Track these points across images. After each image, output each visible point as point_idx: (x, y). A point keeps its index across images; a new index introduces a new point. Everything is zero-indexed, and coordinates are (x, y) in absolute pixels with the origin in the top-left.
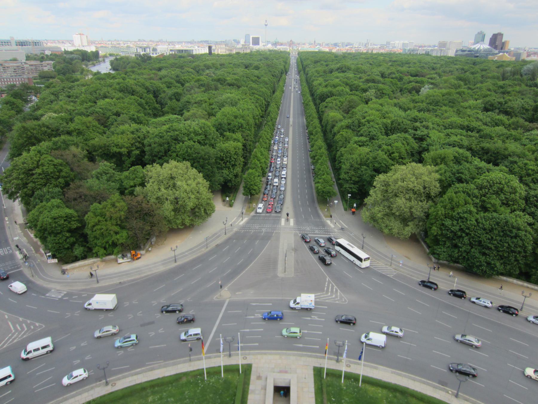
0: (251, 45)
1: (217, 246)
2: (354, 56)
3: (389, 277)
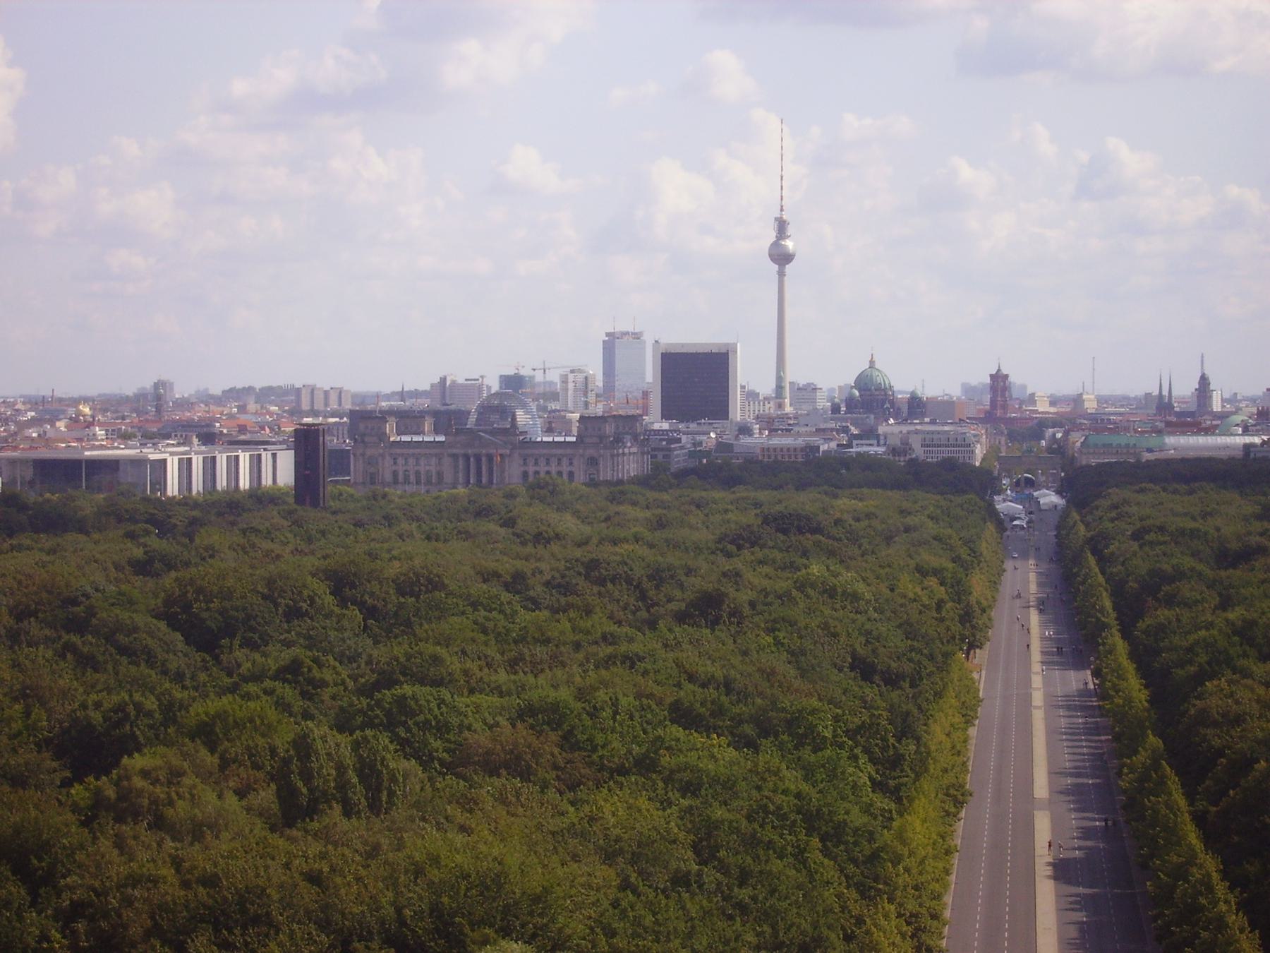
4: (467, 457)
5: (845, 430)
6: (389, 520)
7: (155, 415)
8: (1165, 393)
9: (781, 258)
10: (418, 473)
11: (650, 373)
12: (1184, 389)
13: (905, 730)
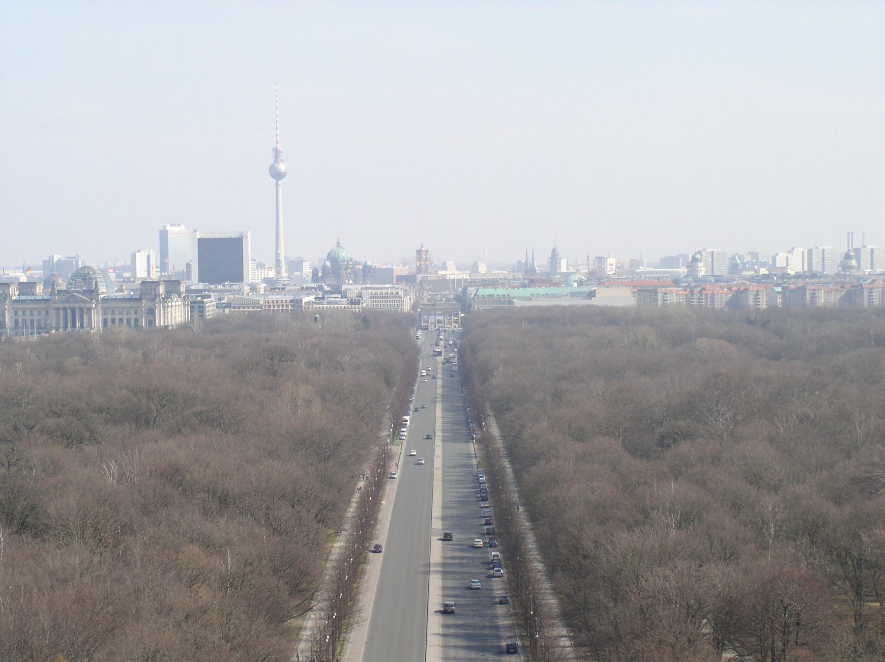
0: (195, 283)
4: (65, 309)
5: (321, 288)
8: (530, 260)
10: (32, 322)
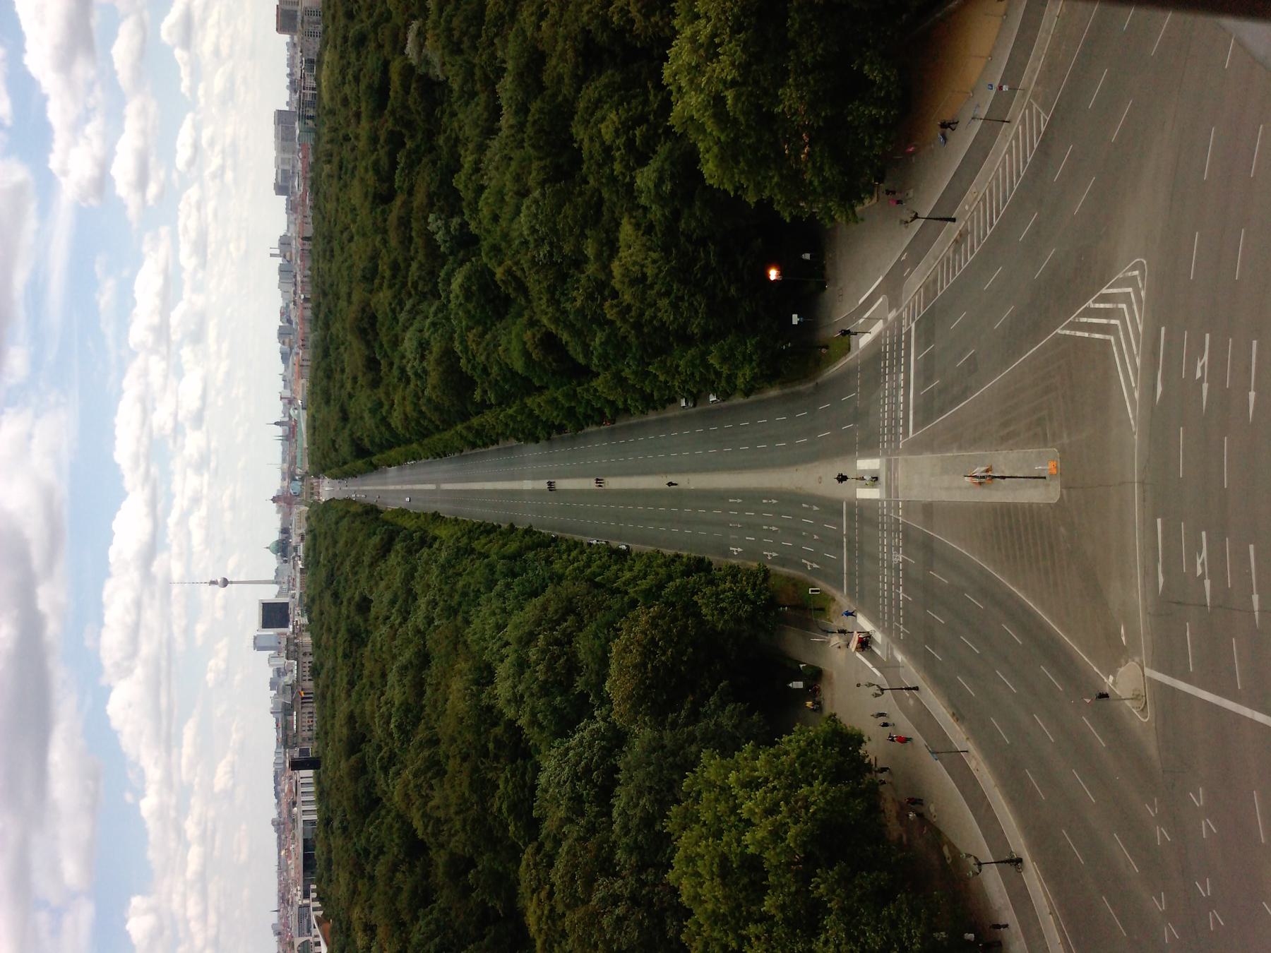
1: (958, 716)
2: (325, 294)
3: (1050, 126)
6: (326, 733)
7: (282, 826)
9: (225, 583)
11: (271, 632)
12: (279, 431)
13: (410, 537)
